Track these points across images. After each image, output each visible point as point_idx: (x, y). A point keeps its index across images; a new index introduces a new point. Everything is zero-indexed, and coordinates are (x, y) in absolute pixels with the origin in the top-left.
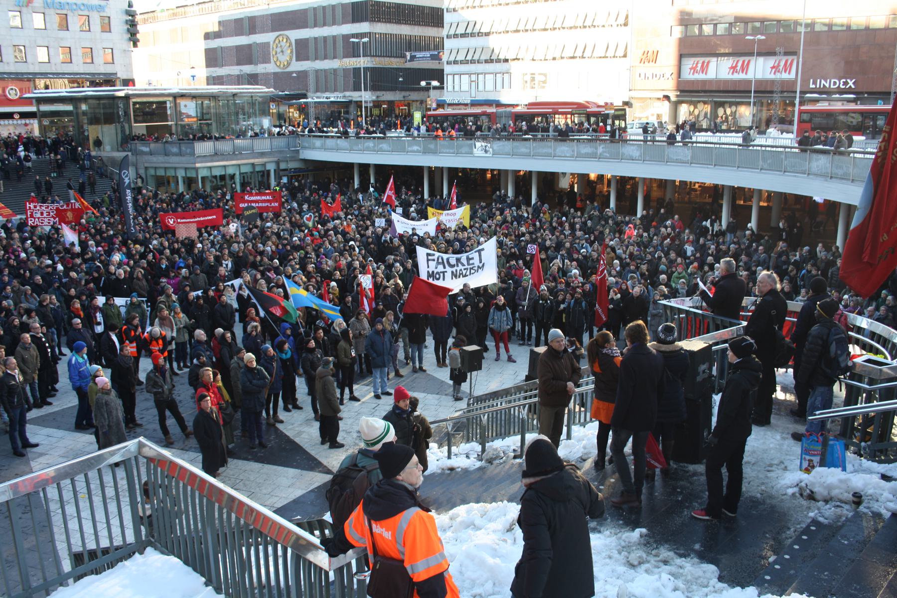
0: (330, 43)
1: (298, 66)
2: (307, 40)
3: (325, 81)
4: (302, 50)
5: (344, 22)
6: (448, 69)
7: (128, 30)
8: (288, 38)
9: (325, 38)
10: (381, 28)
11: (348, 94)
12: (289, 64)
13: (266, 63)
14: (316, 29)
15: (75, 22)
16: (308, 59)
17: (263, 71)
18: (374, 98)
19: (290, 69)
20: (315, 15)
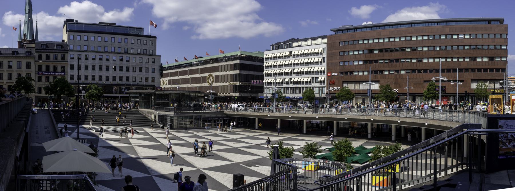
0: (226, 77)
4: (217, 79)
5: (231, 70)
8: (212, 75)
9: (224, 75)
11: (231, 94)
15: (144, 70)
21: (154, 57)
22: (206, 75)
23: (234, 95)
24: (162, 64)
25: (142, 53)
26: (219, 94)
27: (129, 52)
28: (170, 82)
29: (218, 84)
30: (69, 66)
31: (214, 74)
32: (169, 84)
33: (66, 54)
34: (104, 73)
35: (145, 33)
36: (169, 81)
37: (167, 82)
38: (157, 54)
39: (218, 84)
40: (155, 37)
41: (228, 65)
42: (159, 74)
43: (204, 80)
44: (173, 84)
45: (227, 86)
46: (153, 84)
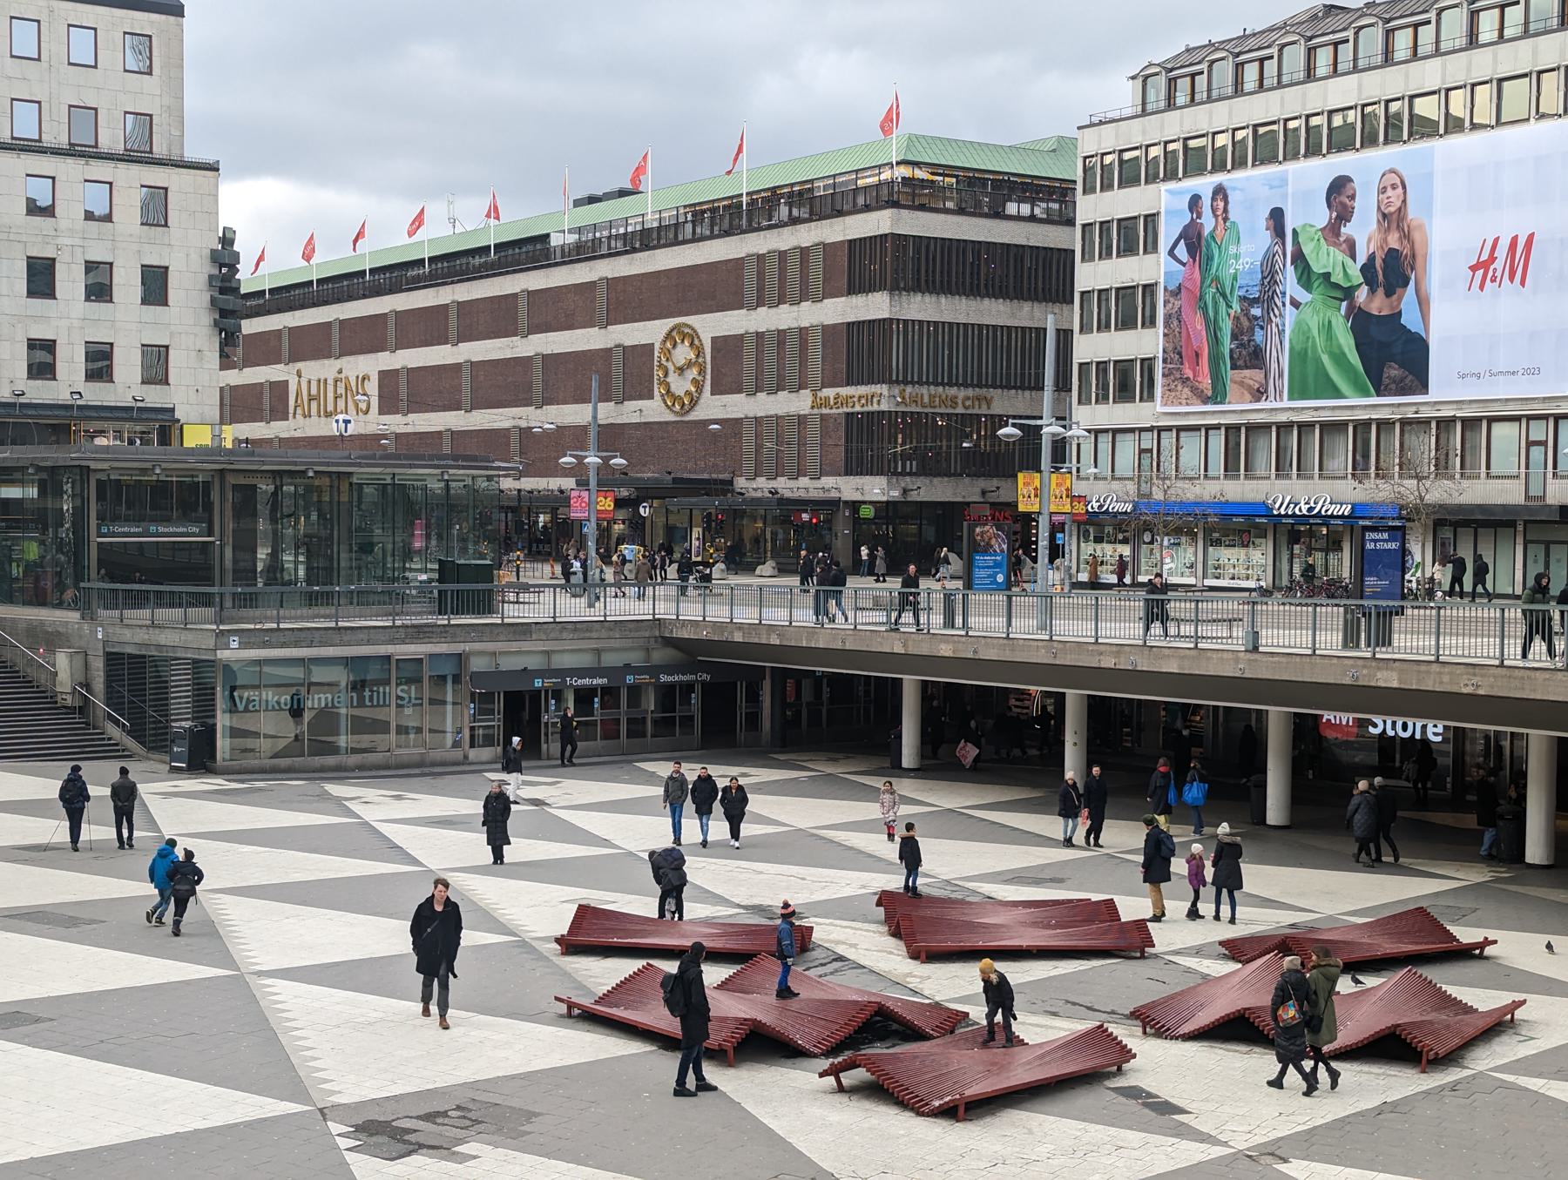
0: (792, 345)
1: (715, 407)
2: (739, 339)
3: (781, 444)
4: (731, 364)
7: (213, 301)
8: (692, 337)
10: (921, 308)
11: (828, 481)
12: (694, 403)
13: (640, 397)
14: (762, 310)
16: (739, 391)
17: (635, 419)
18: (895, 494)
19: (698, 414)
20: (761, 275)
21: (157, 176)
22: (650, 332)
23: (848, 488)
24: (227, 240)
25: (56, 135)
26: (741, 483)
28: (398, 392)
29: (738, 406)
31: (712, 325)
32: (389, 404)
36: (386, 377)
37: (373, 388)
39: (738, 406)
41: (804, 252)
42: (207, 318)
43: (633, 376)
44: (418, 404)
45: (802, 420)
46: (154, 397)
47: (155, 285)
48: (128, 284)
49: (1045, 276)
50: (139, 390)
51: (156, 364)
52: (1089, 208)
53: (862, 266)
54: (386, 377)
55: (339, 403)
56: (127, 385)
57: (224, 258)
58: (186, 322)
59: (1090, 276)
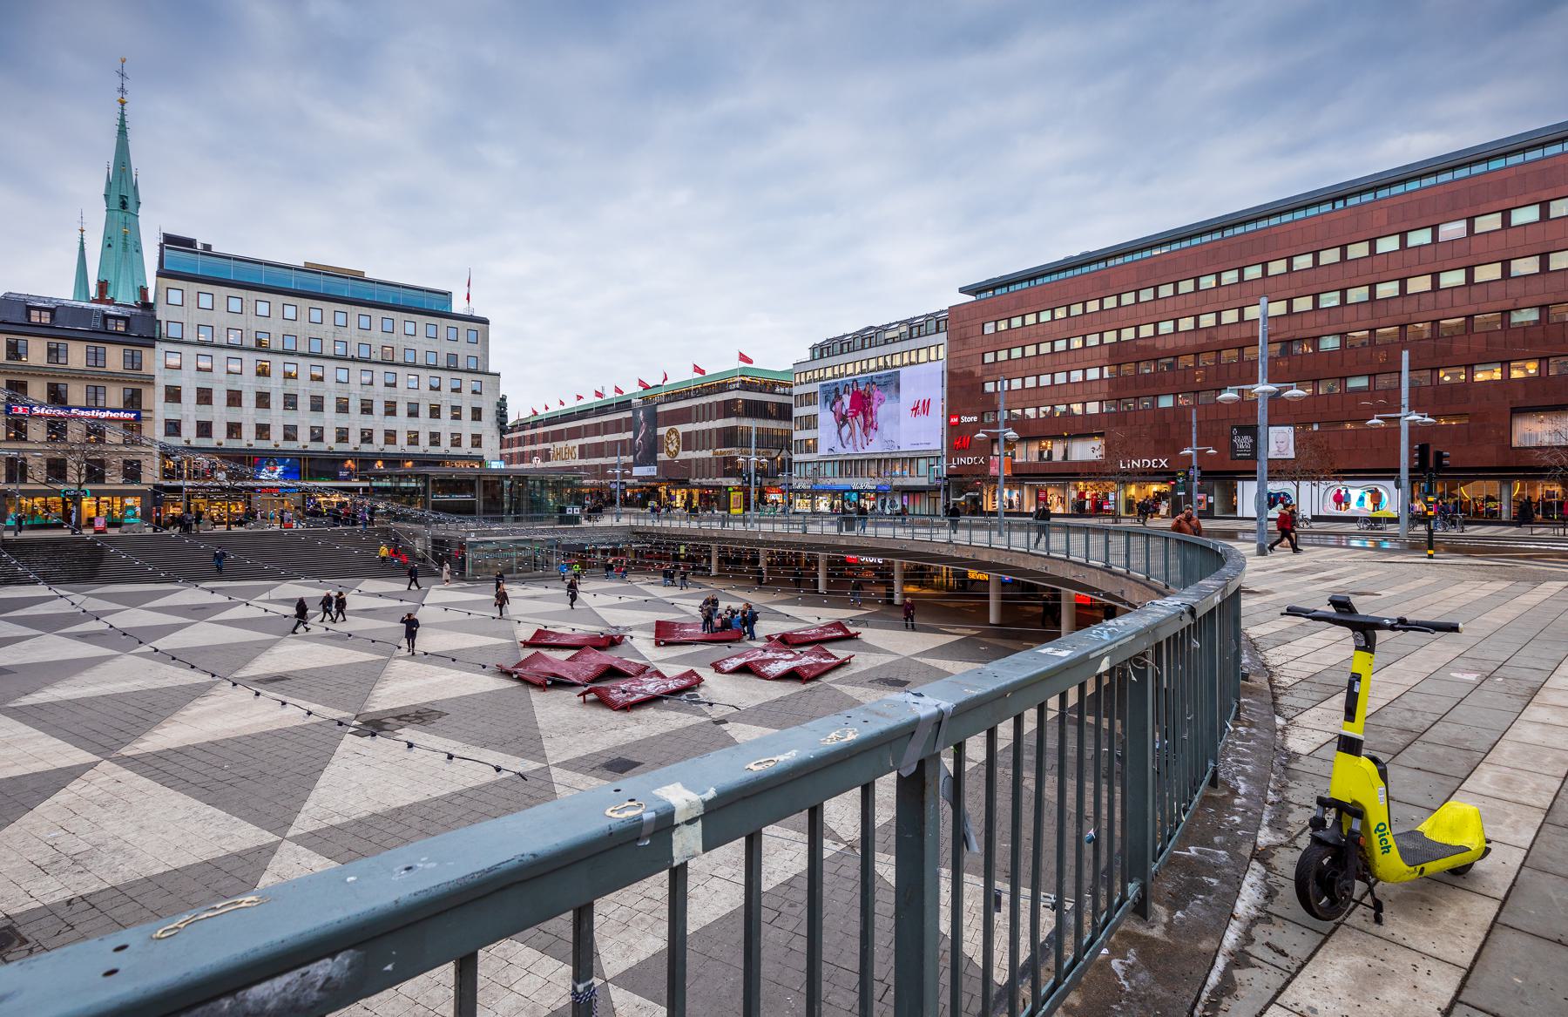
1: (683, 455)
4: (688, 441)
6: (796, 458)
8: (676, 432)
24: (503, 399)
27: (398, 359)
28: (584, 452)
29: (690, 455)
30: (160, 392)
31: (682, 428)
32: (582, 456)
33: (146, 352)
34: (424, 425)
35: (458, 306)
36: (581, 447)
38: (491, 370)
39: (690, 455)
40: (486, 322)
46: (476, 451)
47: (477, 414)
48: (467, 413)
49: (784, 412)
50: (308, 443)
51: (477, 440)
52: (796, 391)
53: (727, 409)
54: (581, 447)
55: (567, 455)
56: (466, 448)
57: (502, 405)
58: (488, 427)
59: (798, 412)
